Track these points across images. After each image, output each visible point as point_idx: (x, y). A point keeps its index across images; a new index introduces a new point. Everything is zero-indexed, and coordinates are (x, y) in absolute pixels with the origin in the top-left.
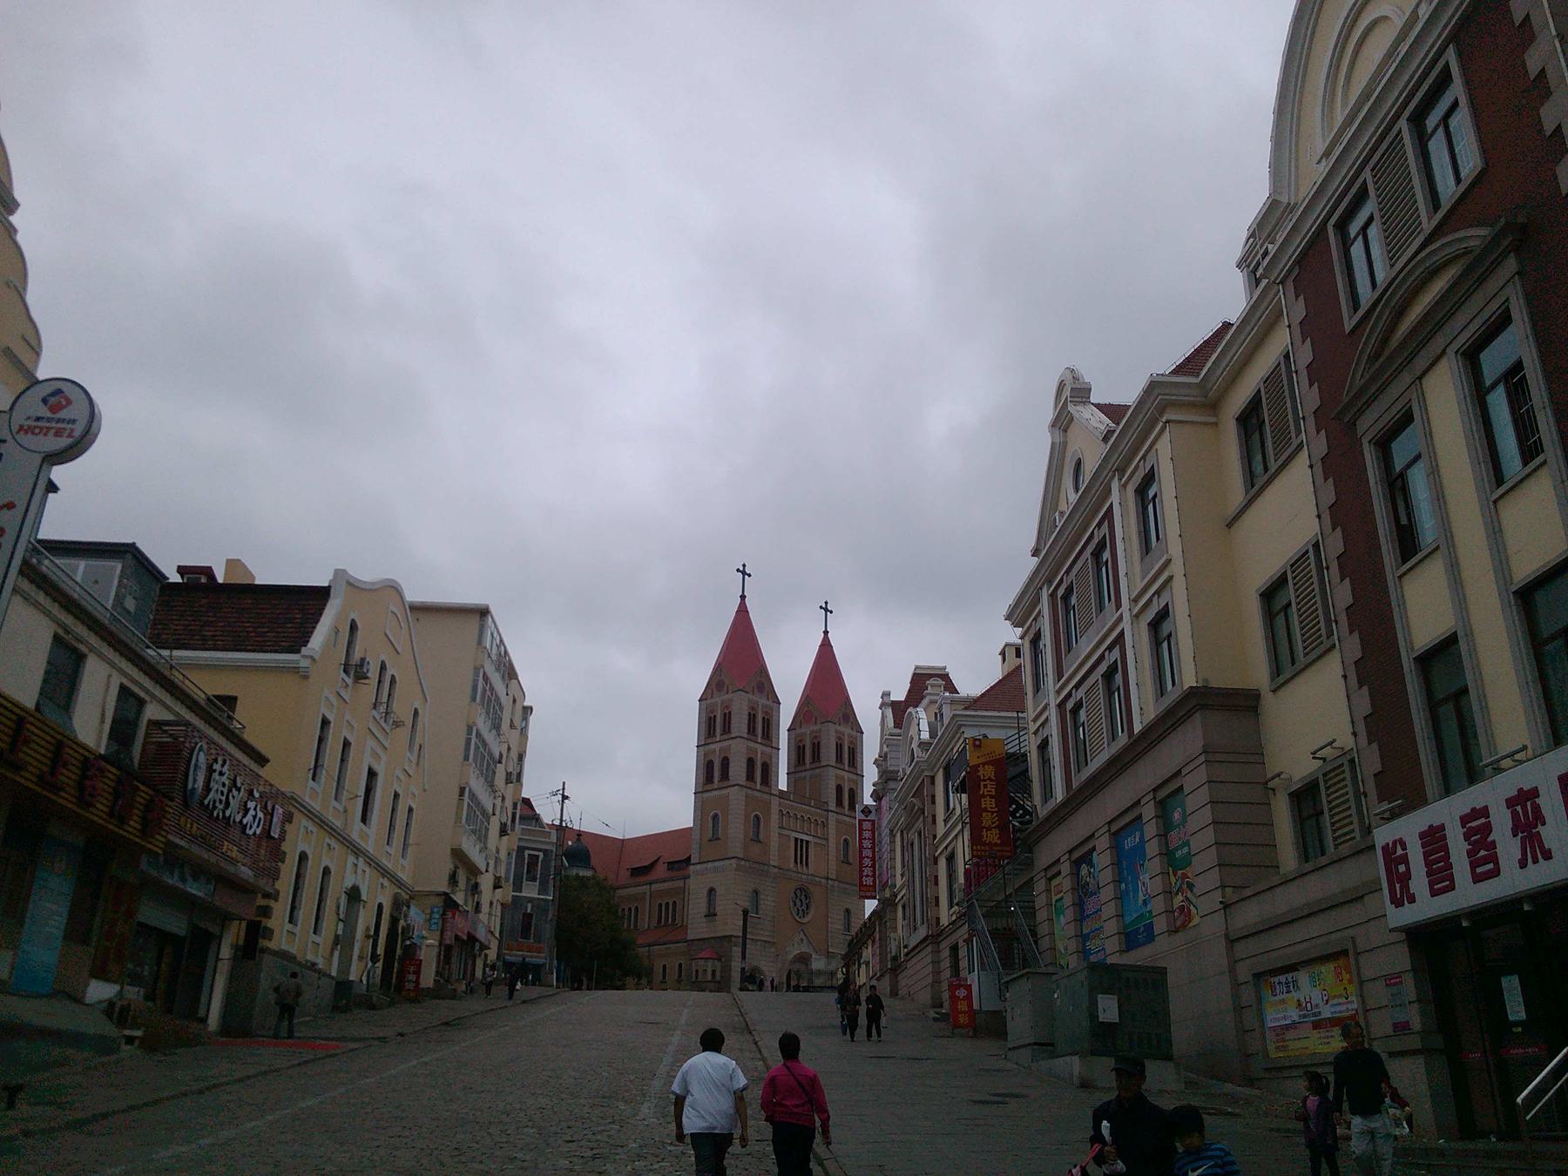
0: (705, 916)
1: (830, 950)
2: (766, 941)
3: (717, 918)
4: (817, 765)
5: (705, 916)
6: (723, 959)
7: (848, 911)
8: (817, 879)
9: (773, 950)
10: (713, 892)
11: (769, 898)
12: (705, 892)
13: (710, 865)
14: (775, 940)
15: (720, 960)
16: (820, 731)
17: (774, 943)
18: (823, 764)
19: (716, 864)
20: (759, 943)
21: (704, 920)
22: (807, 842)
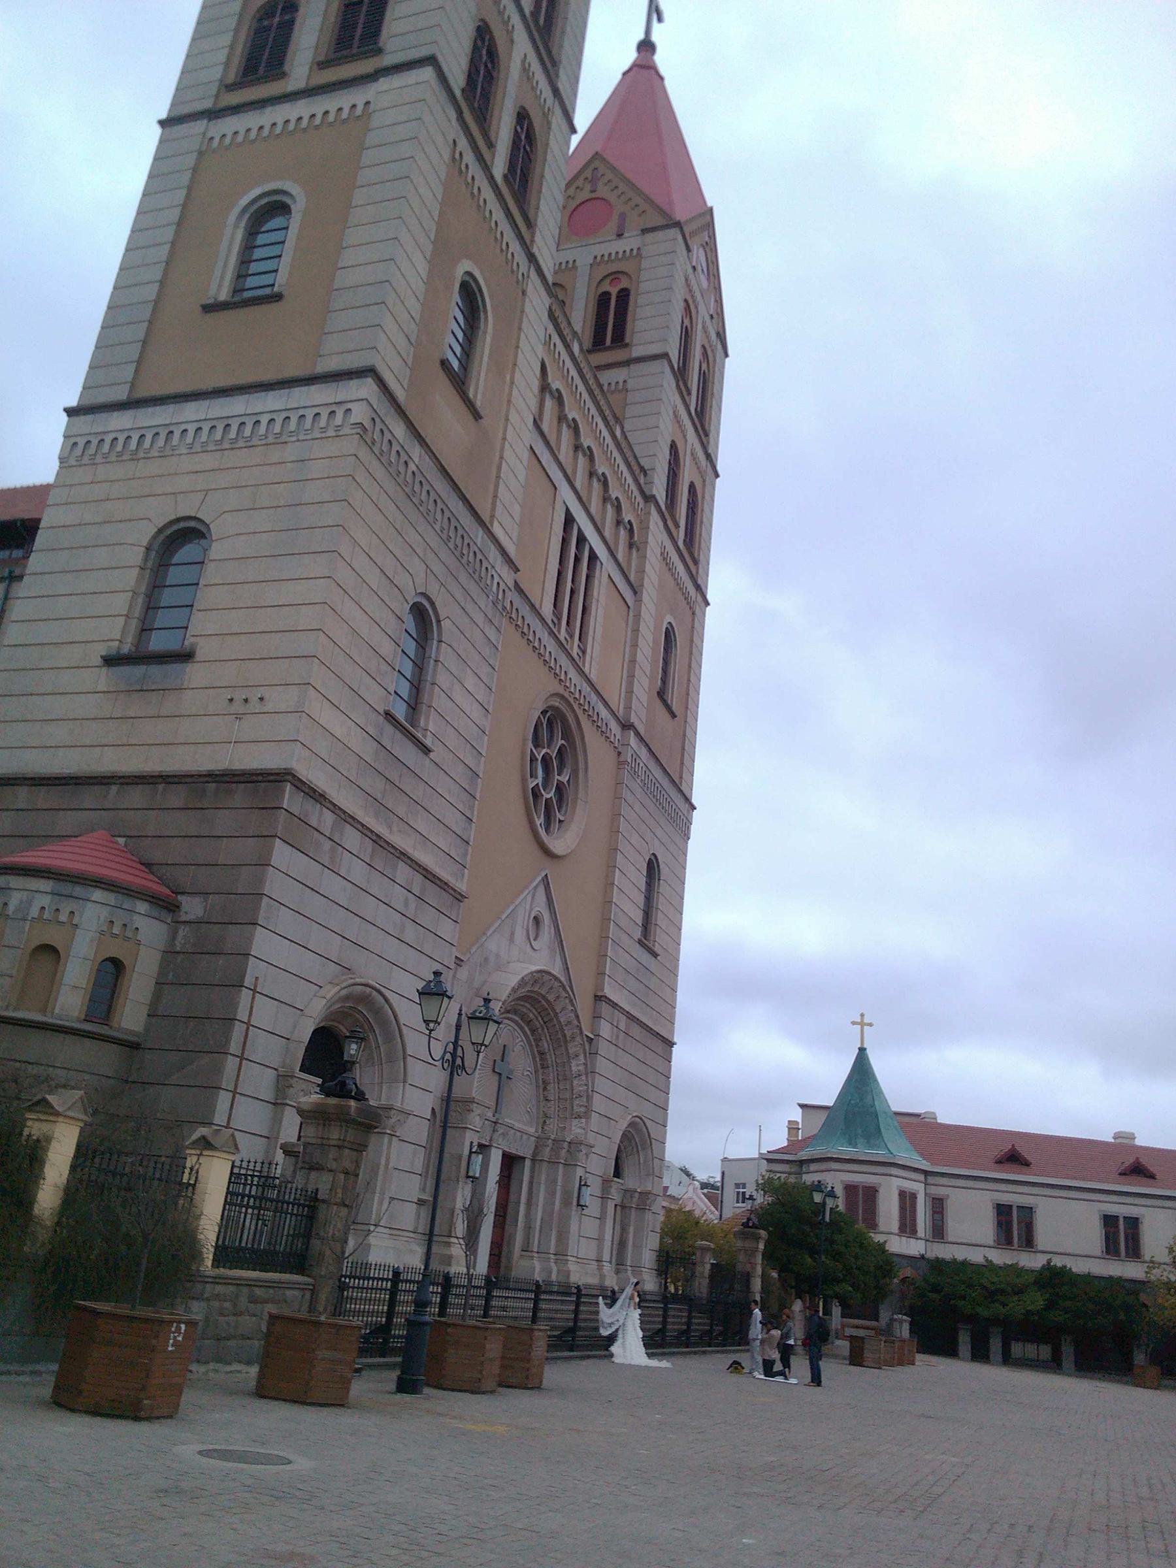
0: (110, 661)
1: (608, 991)
2: (429, 875)
3: (194, 673)
4: (618, 355)
5: (110, 661)
6: (192, 908)
7: (652, 868)
9: (447, 929)
10: (187, 552)
11: (470, 682)
12: (145, 533)
13: (192, 411)
14: (462, 886)
15: (166, 905)
16: (636, 255)
17: (459, 897)
18: (637, 352)
19: (237, 406)
20: (403, 872)
21: (104, 678)
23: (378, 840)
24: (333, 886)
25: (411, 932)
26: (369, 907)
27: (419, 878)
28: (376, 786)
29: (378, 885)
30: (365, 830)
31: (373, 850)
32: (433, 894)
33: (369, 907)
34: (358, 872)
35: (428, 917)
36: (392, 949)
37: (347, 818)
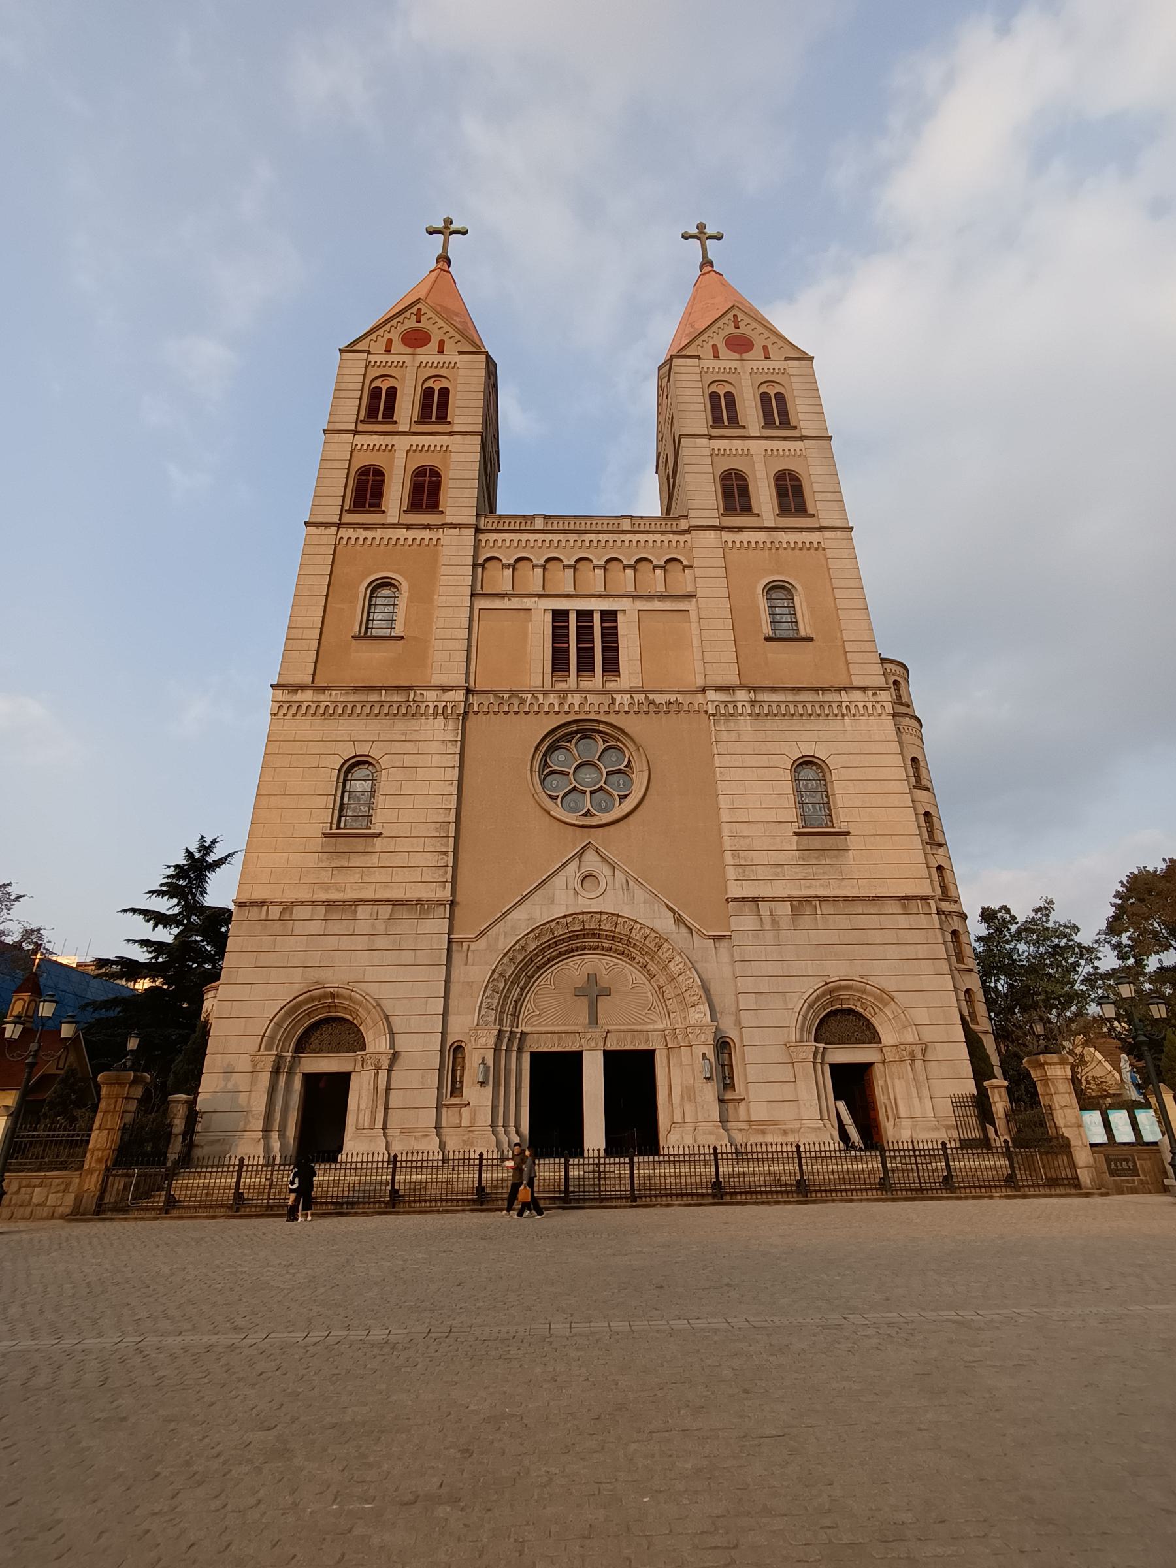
2: (395, 903)
8: (658, 699)
20: (363, 911)
22: (610, 616)
23: (328, 904)
24: (291, 943)
25: (381, 942)
26: (330, 942)
27: (385, 911)
28: (325, 876)
29: (336, 927)
30: (314, 903)
31: (326, 911)
32: (403, 912)
33: (330, 942)
34: (316, 927)
35: (405, 926)
36: (364, 958)
37: (288, 907)
